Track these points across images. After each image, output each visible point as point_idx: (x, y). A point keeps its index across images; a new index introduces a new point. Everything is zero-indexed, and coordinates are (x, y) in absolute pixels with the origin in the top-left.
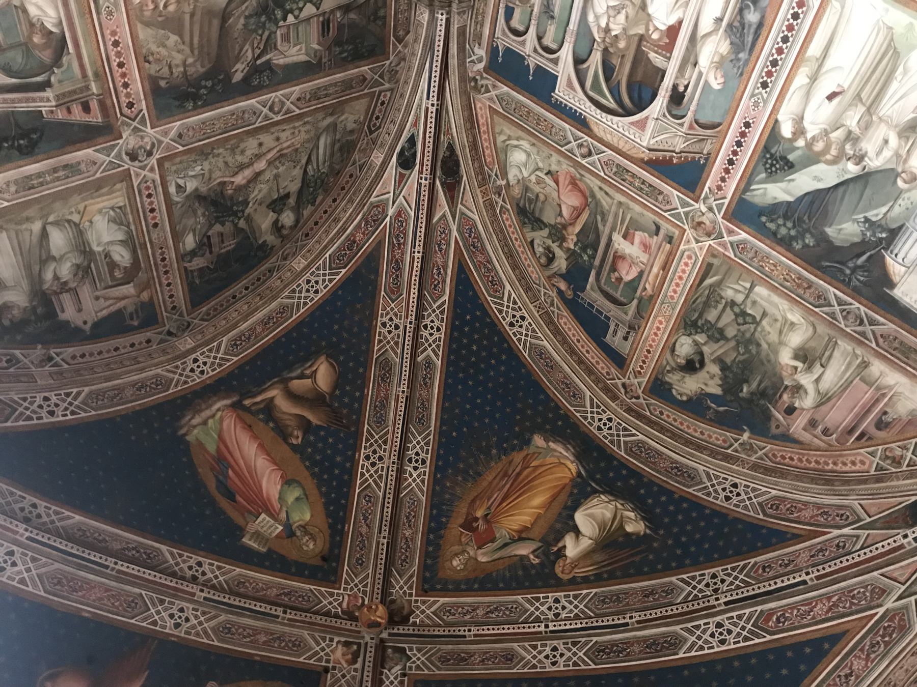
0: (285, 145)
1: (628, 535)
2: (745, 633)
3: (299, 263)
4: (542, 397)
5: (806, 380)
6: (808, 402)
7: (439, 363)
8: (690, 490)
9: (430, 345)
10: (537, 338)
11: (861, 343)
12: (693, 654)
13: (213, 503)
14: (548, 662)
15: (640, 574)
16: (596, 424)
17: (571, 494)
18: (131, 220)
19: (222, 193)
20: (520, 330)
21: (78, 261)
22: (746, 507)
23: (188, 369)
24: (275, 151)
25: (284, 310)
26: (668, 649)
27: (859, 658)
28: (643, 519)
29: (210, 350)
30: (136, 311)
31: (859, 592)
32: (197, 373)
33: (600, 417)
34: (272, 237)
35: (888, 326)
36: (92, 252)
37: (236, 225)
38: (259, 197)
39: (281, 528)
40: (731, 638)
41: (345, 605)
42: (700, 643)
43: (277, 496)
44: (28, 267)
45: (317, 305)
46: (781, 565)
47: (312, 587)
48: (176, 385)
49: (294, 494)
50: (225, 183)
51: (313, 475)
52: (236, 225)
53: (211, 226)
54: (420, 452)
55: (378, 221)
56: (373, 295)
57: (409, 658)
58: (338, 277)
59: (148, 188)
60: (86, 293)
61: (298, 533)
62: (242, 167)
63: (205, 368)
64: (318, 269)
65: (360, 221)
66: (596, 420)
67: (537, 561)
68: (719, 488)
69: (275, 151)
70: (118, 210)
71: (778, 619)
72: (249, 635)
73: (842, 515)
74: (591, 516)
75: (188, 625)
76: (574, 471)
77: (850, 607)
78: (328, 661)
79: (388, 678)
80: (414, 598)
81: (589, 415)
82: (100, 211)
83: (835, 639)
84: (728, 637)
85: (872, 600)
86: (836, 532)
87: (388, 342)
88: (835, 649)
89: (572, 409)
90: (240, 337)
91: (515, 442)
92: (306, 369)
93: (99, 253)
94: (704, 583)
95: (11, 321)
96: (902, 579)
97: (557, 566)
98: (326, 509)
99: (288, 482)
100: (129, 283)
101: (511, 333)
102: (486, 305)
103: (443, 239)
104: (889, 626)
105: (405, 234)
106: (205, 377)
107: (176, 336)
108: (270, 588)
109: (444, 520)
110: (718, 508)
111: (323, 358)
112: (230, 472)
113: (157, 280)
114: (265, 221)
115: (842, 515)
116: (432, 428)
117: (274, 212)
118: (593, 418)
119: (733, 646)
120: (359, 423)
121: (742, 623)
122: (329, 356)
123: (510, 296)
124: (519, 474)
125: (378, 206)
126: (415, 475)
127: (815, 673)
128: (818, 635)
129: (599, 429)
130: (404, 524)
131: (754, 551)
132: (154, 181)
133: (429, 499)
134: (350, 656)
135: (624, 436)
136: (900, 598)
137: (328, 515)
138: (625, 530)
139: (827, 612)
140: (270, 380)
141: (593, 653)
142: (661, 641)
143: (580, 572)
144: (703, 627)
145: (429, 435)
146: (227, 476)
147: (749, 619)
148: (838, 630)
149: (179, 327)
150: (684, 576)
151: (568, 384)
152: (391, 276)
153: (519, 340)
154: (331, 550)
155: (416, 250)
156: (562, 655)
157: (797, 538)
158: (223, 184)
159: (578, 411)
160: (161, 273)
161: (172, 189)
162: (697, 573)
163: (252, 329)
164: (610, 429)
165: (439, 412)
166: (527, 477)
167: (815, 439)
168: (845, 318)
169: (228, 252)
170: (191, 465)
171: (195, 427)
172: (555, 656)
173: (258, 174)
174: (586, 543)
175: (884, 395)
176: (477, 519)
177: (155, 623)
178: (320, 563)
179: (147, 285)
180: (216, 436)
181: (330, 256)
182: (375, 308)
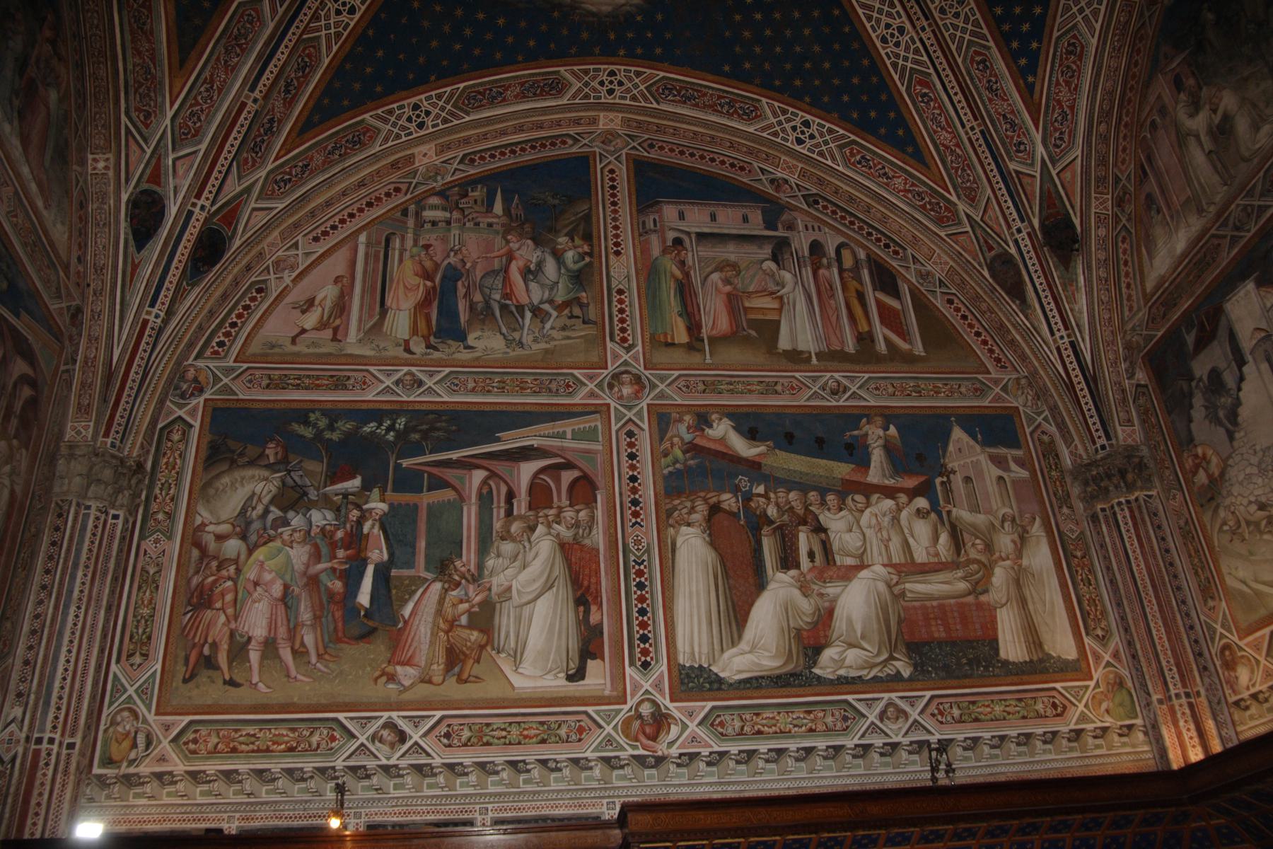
2: (901, 62)
5: (1199, 123)
6: (1182, 115)
11: (1219, 215)
27: (905, 184)
31: (968, 175)
35: (1226, 257)
40: (891, 48)
42: (875, 15)
73: (1061, 139)
77: (953, 168)
83: (919, 157)
84: (891, 44)
86: (1038, 138)
96: (986, 218)
104: (940, 208)
115: (1061, 139)
121: (911, 56)
128: (919, 139)
131: (1003, 40)
136: (968, 216)
139: (943, 145)
144: (894, 11)
147: (916, 62)
157: (1028, 92)
167: (1148, 108)
168: (1246, 207)
175: (1172, 217)
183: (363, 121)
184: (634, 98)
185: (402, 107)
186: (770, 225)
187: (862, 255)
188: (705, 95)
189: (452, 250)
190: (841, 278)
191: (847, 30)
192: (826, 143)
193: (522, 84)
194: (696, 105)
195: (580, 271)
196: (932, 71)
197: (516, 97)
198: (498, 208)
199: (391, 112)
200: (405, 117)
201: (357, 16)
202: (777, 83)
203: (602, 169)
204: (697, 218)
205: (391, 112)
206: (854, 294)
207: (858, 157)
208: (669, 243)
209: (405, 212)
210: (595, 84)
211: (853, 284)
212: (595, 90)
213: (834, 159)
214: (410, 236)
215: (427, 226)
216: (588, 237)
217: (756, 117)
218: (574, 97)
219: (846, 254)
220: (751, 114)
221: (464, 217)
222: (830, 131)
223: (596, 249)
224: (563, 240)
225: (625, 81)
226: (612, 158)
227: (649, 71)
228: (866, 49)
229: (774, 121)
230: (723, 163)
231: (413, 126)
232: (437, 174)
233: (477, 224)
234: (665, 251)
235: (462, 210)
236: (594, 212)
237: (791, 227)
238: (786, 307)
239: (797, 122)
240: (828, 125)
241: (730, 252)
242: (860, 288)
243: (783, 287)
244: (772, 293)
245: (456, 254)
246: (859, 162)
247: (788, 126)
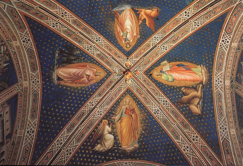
7: (175, 141)
9: (182, 143)
14: (91, 102)
17: (118, 140)
32: (217, 80)
39: (164, 70)
41: (138, 71)
47: (147, 68)
49: (170, 79)
51: (172, 86)
54: (158, 115)
61: (160, 73)
67: (112, 118)
87: (191, 133)
89: (136, 162)
98: (161, 83)
99: (174, 80)
106: (215, 80)
109: (139, 106)
111: (200, 113)
116: (161, 123)
120: (176, 106)
122: (199, 115)
133: (146, 107)
137: (160, 82)
140: (203, 95)
143: (102, 125)
145: (160, 120)
146: (184, 68)
154: (152, 77)
156: (90, 105)
166: (131, 134)
170: (191, 62)
172: (91, 104)
174: (106, 132)
178: (151, 73)
180: (196, 72)
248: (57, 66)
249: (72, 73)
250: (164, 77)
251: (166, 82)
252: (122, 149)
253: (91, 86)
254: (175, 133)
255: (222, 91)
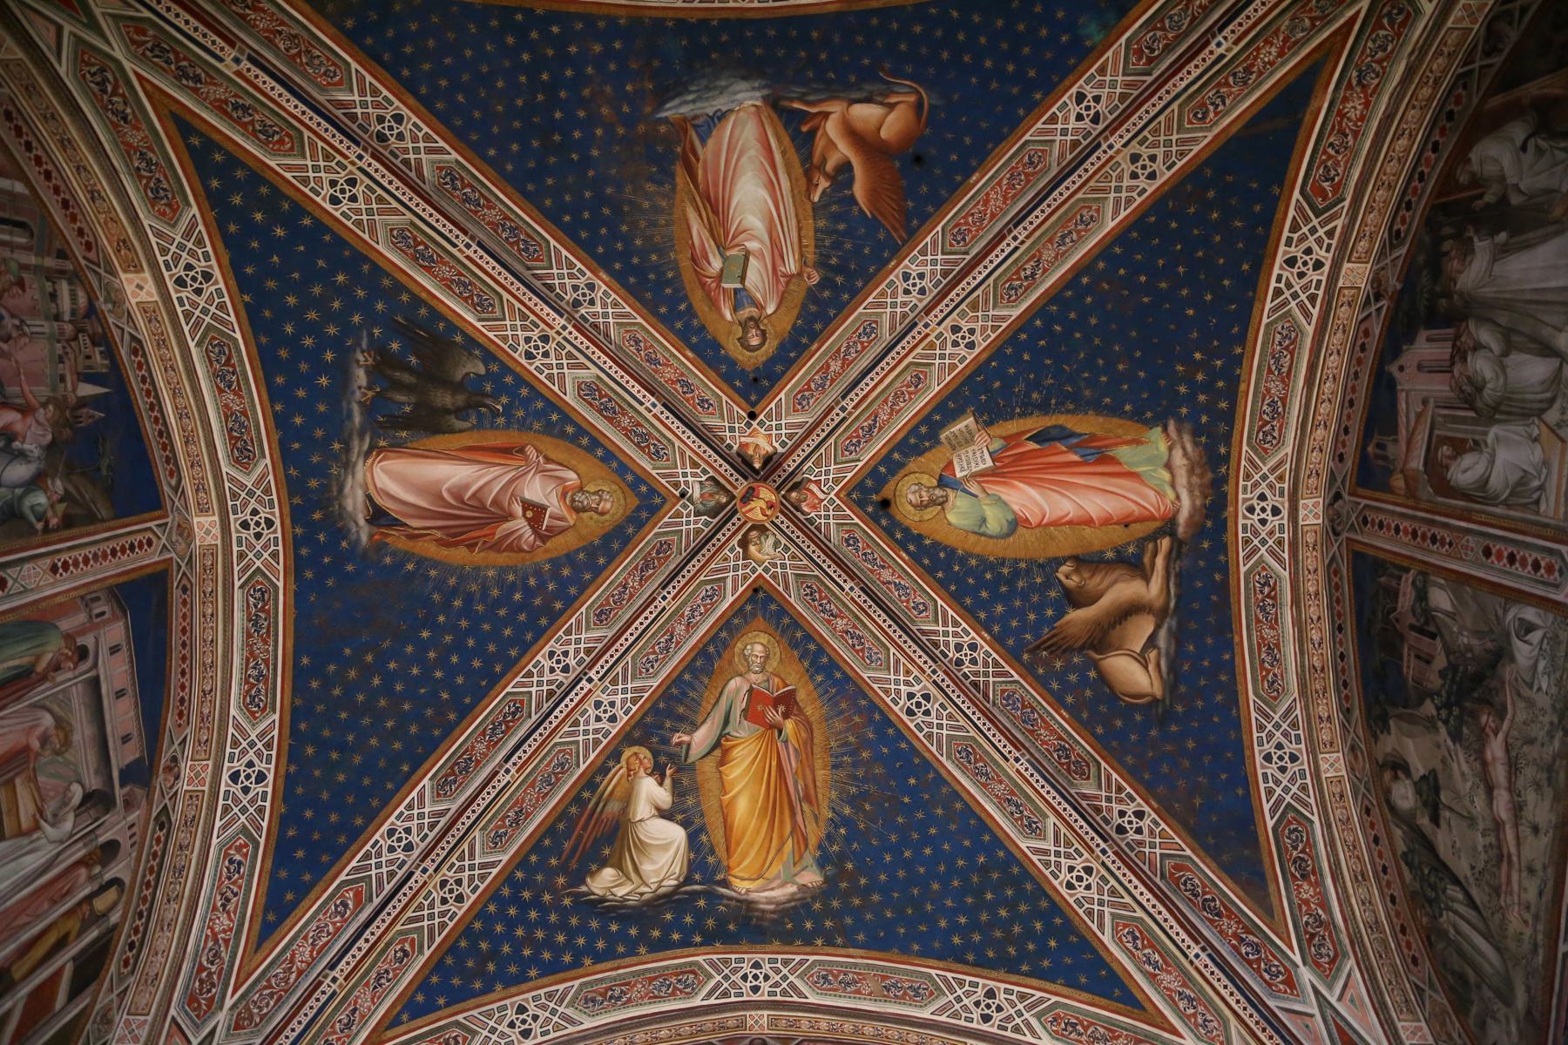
0: (1515, 876)
1: (604, 863)
2: (373, 861)
3: (1334, 765)
4: (861, 937)
7: (1023, 846)
8: (577, 983)
9: (1058, 854)
10: (942, 1010)
12: (414, 794)
13: (1044, 408)
14: (559, 649)
15: (549, 829)
16: (766, 968)
17: (712, 852)
18: (1512, 513)
19: (1491, 704)
20: (974, 998)
21: (1487, 392)
22: (489, 1015)
23: (1268, 494)
24: (1513, 850)
25: (1274, 690)
26: (447, 775)
27: (224, 931)
28: (603, 900)
29: (1280, 542)
30: (1385, 458)
32: (1255, 502)
33: (770, 982)
34: (1389, 749)
36: (1491, 421)
37: (1432, 694)
38: (1455, 766)
39: (959, 475)
40: (385, 844)
41: (813, 487)
42: (416, 812)
43: (1004, 497)
44: (1508, 306)
45: (1246, 743)
46: (387, 972)
47: (860, 464)
48: (1251, 462)
49: (995, 522)
50: (1502, 719)
52: (1432, 694)
53: (1448, 651)
54: (927, 719)
55: (1308, 940)
56: (1196, 833)
57: (698, 514)
58: (1267, 807)
59: (1550, 569)
60: (1439, 387)
61: (938, 492)
62: (1513, 767)
63: (1256, 517)
64: (1304, 788)
65: (1328, 910)
66: (771, 973)
67: (675, 739)
68: (543, 1015)
69: (1513, 850)
70: (1535, 496)
71: (345, 905)
72: (847, 353)
74: (665, 848)
75: (900, 291)
76: (736, 883)
77: (268, 981)
78: (761, 424)
79: (694, 475)
80: (760, 570)
81: (785, 971)
82: (1546, 463)
83: (267, 931)
85: (247, 1008)
87: (1109, 799)
88: (259, 919)
89: (812, 958)
90: (1274, 598)
91: (835, 848)
92: (1159, 654)
93: (1486, 433)
94: (465, 882)
95: (1447, 253)
97: (649, 755)
98: (945, 548)
99: (1016, 523)
100: (1425, 464)
101: (981, 981)
102: (1048, 985)
103: (1194, 1015)
104: (209, 991)
105: (1250, 963)
106: (1242, 509)
107: (1331, 505)
108: (891, 414)
109: (819, 678)
110: (524, 987)
111: (1157, 690)
112: (1075, 458)
113: (1410, 512)
114: (1417, 750)
116: (943, 759)
117: (1424, 777)
118: (778, 971)
119: (377, 836)
120: (1028, 670)
121: (384, 870)
122: (1155, 701)
123: (1033, 1032)
124: (793, 814)
125: (1332, 961)
126: (902, 687)
127: (266, 877)
128: (288, 922)
129: (757, 965)
130: (854, 626)
131: (436, 965)
132: (1556, 586)
133: (859, 681)
134: (751, 452)
135: (718, 985)
137: (936, 545)
138: (612, 866)
139: (293, 956)
140: (1178, 597)
141: (522, 702)
142: (460, 779)
143: (618, 773)
145: (940, 747)
146: (1071, 449)
148: (267, 945)
149: (1339, 515)
150: (495, 871)
151: (849, 985)
152: (1204, 886)
153: (961, 983)
154: (891, 518)
155: (1203, 956)
156: (552, 670)
157: (392, 1022)
158: (1501, 714)
159: (801, 963)
160: (1416, 525)
161: (1530, 614)
162: (482, 887)
163: (1274, 623)
164: (745, 978)
165: (957, 787)
166: (782, 822)
169: (1401, 658)
170: (1115, 411)
171: (1170, 449)
172: (558, 662)
173: (1490, 790)
174: (642, 810)
176: (786, 716)
177: (923, 252)
178: (887, 492)
179: (1411, 492)
181: (1312, 822)
182: (1175, 823)
183: (189, 205)
184: (242, 556)
185: (207, 257)
186: (128, 775)
187: (114, 918)
188: (265, 642)
189: (22, 321)
190: (79, 904)
191: (389, 786)
192: (244, 810)
193: (244, 413)
194: (249, 635)
195: (21, 517)
196: (376, 901)
197: (226, 406)
198: (87, 390)
199: (200, 242)
200: (193, 261)
201: (328, 206)
202: (303, 726)
203: (150, 529)
204: (116, 671)
205: (200, 242)
206: (62, 933)
207: (238, 857)
208: (80, 641)
209: (62, 255)
210: (253, 504)
211: (74, 925)
212: (245, 505)
213: (224, 828)
214: (33, 260)
215: (49, 287)
216: (68, 522)
217: (253, 713)
218: (232, 479)
219: (111, 894)
220: (254, 706)
221: (68, 341)
222: (261, 810)
223: (54, 536)
224: (59, 486)
225: (263, 540)
226: (164, 540)
227: (281, 567)
228: (373, 817)
229: (253, 737)
230: (183, 687)
231: (179, 271)
232: (114, 303)
233: (61, 361)
234: (69, 637)
235: (76, 338)
236: (99, 526)
237: (129, 805)
238: (25, 841)
239: (260, 766)
240: (268, 804)
241: (82, 731)
242: (72, 937)
243: (53, 825)
244: (41, 812)
245: (18, 328)
246: (231, 862)
247: (251, 755)
248: (362, 439)
249: (449, 490)
250: (959, 513)
251: (972, 538)
252: (733, 894)
253: (556, 563)
254: (1017, 806)
255: (1280, 561)
